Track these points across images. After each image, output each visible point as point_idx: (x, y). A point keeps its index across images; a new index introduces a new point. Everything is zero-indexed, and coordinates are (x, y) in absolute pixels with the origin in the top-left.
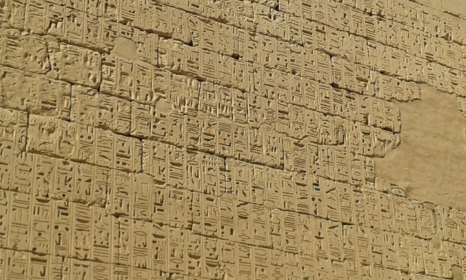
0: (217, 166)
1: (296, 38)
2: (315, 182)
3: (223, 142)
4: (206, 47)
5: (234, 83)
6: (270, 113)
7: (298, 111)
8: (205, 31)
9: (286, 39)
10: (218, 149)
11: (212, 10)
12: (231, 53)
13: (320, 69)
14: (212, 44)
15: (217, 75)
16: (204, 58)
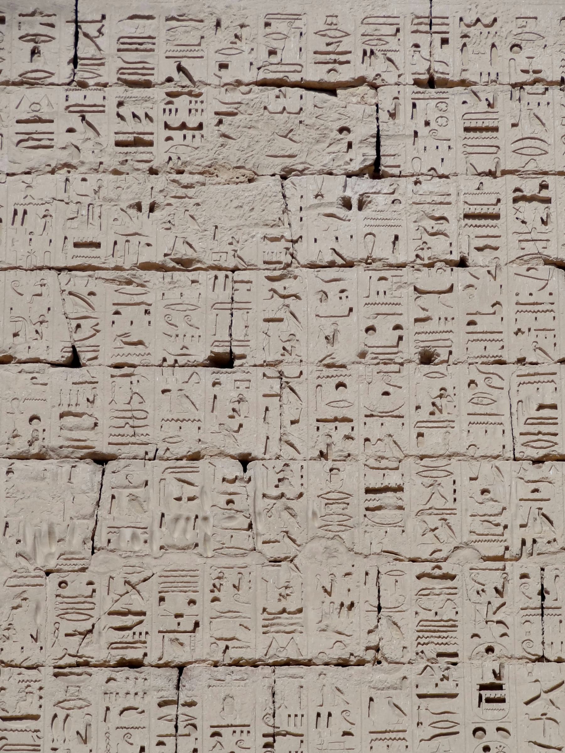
0: (154, 698)
1: (439, 248)
2: (490, 679)
3: (172, 623)
4: (119, 360)
5: (215, 440)
6: (336, 501)
7: (434, 474)
8: (117, 313)
9: (401, 259)
10: (155, 649)
11: (144, 240)
12: (202, 356)
13: (526, 321)
14: (140, 343)
15: (155, 434)
16: (113, 393)
